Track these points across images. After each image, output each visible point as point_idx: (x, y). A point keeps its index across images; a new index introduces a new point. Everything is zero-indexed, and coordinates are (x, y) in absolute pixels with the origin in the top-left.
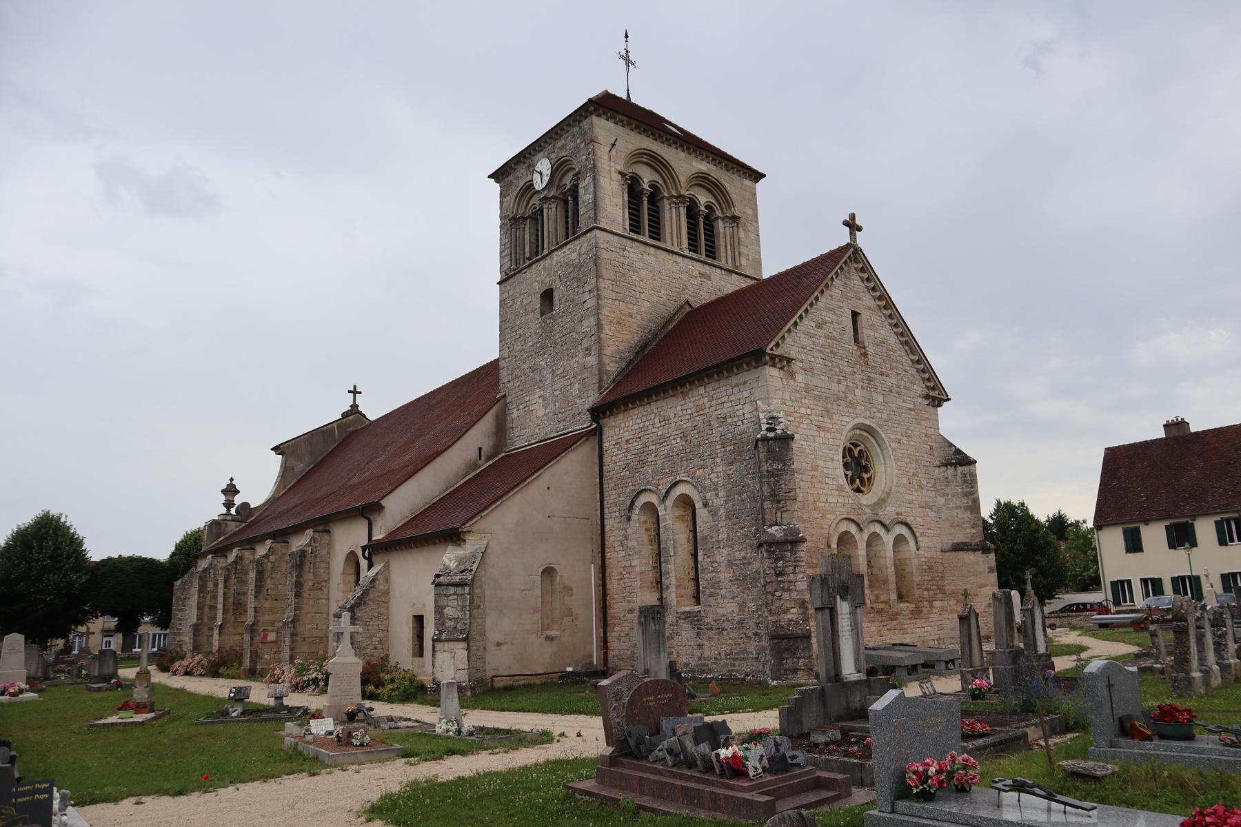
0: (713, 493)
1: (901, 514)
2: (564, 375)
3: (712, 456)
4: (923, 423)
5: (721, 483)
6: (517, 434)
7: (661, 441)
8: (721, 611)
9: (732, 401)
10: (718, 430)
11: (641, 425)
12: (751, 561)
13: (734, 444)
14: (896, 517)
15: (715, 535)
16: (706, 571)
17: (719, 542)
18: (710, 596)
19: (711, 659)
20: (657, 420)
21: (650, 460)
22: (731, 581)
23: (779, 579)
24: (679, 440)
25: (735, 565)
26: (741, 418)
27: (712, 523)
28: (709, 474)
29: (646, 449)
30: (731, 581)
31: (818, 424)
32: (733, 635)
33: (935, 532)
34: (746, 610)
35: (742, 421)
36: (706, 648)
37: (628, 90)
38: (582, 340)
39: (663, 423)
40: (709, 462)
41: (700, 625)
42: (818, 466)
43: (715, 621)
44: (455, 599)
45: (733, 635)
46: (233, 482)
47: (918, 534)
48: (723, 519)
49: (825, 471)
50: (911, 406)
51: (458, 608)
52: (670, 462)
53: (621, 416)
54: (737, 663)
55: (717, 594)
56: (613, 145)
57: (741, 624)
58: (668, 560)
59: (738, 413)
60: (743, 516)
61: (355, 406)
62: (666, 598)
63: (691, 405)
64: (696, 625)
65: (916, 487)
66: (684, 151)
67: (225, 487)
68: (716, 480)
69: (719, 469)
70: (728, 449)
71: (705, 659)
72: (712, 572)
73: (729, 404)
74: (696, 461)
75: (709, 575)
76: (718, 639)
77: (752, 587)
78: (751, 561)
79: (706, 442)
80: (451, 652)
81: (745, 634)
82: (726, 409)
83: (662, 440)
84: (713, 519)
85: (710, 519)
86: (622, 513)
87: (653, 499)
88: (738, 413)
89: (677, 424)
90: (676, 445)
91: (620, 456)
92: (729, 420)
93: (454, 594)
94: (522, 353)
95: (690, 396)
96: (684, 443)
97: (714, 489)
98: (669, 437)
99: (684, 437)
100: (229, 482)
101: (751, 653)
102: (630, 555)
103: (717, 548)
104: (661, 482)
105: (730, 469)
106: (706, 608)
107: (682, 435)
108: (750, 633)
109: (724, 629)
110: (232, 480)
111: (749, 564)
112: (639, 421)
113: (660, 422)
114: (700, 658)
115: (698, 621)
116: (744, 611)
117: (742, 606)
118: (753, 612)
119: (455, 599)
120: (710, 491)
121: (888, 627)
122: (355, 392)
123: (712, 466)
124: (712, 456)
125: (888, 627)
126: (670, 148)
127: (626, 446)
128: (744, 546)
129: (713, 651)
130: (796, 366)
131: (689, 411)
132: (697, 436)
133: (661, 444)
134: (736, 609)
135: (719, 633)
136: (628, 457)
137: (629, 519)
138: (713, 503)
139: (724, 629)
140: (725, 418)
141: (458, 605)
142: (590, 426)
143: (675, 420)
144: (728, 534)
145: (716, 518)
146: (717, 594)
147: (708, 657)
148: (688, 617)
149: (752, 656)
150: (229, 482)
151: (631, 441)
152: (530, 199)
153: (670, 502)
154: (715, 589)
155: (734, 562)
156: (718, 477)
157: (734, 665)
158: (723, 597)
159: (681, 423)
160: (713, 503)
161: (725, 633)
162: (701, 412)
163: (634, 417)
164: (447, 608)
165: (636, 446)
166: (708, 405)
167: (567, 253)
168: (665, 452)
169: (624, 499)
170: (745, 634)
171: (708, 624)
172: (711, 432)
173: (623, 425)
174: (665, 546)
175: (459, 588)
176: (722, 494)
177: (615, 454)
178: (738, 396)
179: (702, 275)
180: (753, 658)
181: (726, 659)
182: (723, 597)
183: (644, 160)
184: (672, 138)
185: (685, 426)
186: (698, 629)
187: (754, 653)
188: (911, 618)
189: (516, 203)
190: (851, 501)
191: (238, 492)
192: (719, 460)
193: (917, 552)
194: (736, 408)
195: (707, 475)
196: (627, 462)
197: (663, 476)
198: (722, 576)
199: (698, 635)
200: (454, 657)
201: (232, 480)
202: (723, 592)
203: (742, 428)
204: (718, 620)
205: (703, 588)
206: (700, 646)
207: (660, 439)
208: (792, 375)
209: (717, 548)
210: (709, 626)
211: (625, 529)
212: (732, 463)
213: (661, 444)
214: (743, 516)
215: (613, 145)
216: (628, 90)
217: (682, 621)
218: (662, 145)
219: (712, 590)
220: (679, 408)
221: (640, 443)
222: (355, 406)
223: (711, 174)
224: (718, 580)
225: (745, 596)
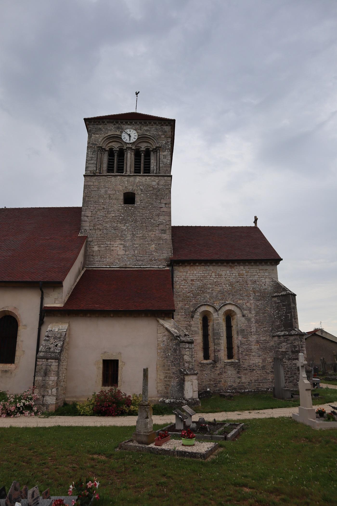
0: (248, 311)
2: (143, 238)
3: (247, 296)
5: (252, 308)
6: (97, 260)
7: (216, 284)
8: (252, 362)
9: (259, 276)
10: (250, 286)
11: (202, 275)
12: (269, 341)
13: (260, 293)
15: (249, 329)
16: (244, 344)
17: (251, 332)
18: (246, 355)
19: (246, 383)
20: (213, 274)
21: (209, 291)
22: (258, 349)
23: (302, 349)
24: (227, 286)
25: (260, 342)
26: (264, 283)
27: (247, 324)
28: (246, 303)
29: (206, 286)
30: (258, 349)
32: (259, 372)
34: (267, 361)
35: (265, 284)
36: (243, 378)
38: (159, 225)
39: (217, 277)
40: (246, 298)
41: (240, 368)
43: (249, 366)
44: (188, 351)
45: (259, 372)
48: (254, 322)
51: (190, 356)
52: (222, 295)
53: (188, 268)
54: (261, 384)
55: (250, 355)
57: (263, 367)
58: (220, 338)
59: (262, 281)
60: (265, 323)
62: (217, 356)
63: (236, 272)
64: (237, 368)
68: (250, 306)
69: (251, 302)
70: (257, 294)
71: (242, 383)
72: (247, 345)
73: (258, 276)
74: (238, 296)
75: (245, 346)
76: (250, 374)
77: (270, 352)
78: (269, 341)
79: (244, 289)
80: (191, 381)
81: (266, 372)
82: (256, 278)
83: (217, 284)
84: (248, 322)
85: (246, 322)
86: (188, 314)
87: (210, 309)
88: (262, 281)
89: (227, 279)
90: (226, 288)
91: (186, 286)
92: (258, 283)
93: (188, 348)
94: (105, 218)
95: (235, 268)
96: (231, 288)
97: (249, 310)
98: (221, 283)
99: (231, 284)
101: (269, 380)
102: (192, 334)
103: (250, 335)
104: (215, 302)
105: (258, 303)
106: (243, 361)
107: (230, 284)
108: (268, 371)
109: (253, 370)
111: (268, 342)
112: (201, 272)
113: (216, 276)
114: (239, 383)
115: (238, 366)
116: (265, 362)
117: (264, 360)
118: (270, 362)
119: (188, 351)
120: (246, 310)
123: (248, 300)
124: (248, 296)
127: (191, 282)
128: (265, 335)
129: (247, 380)
131: (234, 275)
132: (239, 286)
133: (215, 285)
134: (261, 361)
135: (251, 372)
136: (193, 288)
137: (192, 317)
138: (248, 315)
139: (253, 370)
140: (255, 281)
141: (190, 354)
142: (165, 268)
143: (226, 277)
144: (257, 329)
145: (250, 322)
146: (250, 355)
147: (244, 382)
148: (232, 365)
149: (269, 381)
151: (195, 280)
152: (108, 144)
153: (221, 312)
154: (249, 352)
155: (260, 341)
156: (251, 305)
157: (260, 385)
158: (253, 356)
159: (229, 279)
160: (248, 315)
161: (254, 371)
162: (242, 277)
163: (197, 270)
164: (185, 356)
165: (199, 283)
166: (246, 274)
167: (148, 180)
168: (219, 289)
169: (188, 307)
170: (266, 372)
171: (244, 368)
172: (247, 286)
173: (189, 272)
174: (218, 332)
175: (190, 345)
176: (253, 312)
177: (182, 284)
178: (262, 274)
180: (270, 382)
181: (255, 382)
182: (253, 356)
185: (231, 280)
186: (239, 370)
187: (271, 379)
189: (103, 141)
192: (252, 298)
194: (261, 279)
195: (244, 304)
196: (192, 290)
197: (217, 300)
198: (253, 347)
199: (238, 372)
200: (192, 384)
202: (254, 354)
203: (264, 287)
204: (250, 366)
205: (242, 352)
206: (239, 378)
207: (215, 283)
209: (250, 335)
210: (245, 369)
211: (190, 322)
212: (259, 301)
213: (215, 285)
214: (265, 323)
217: (228, 366)
219: (247, 353)
220: (228, 272)
221: (201, 282)
224: (250, 348)
225: (266, 356)
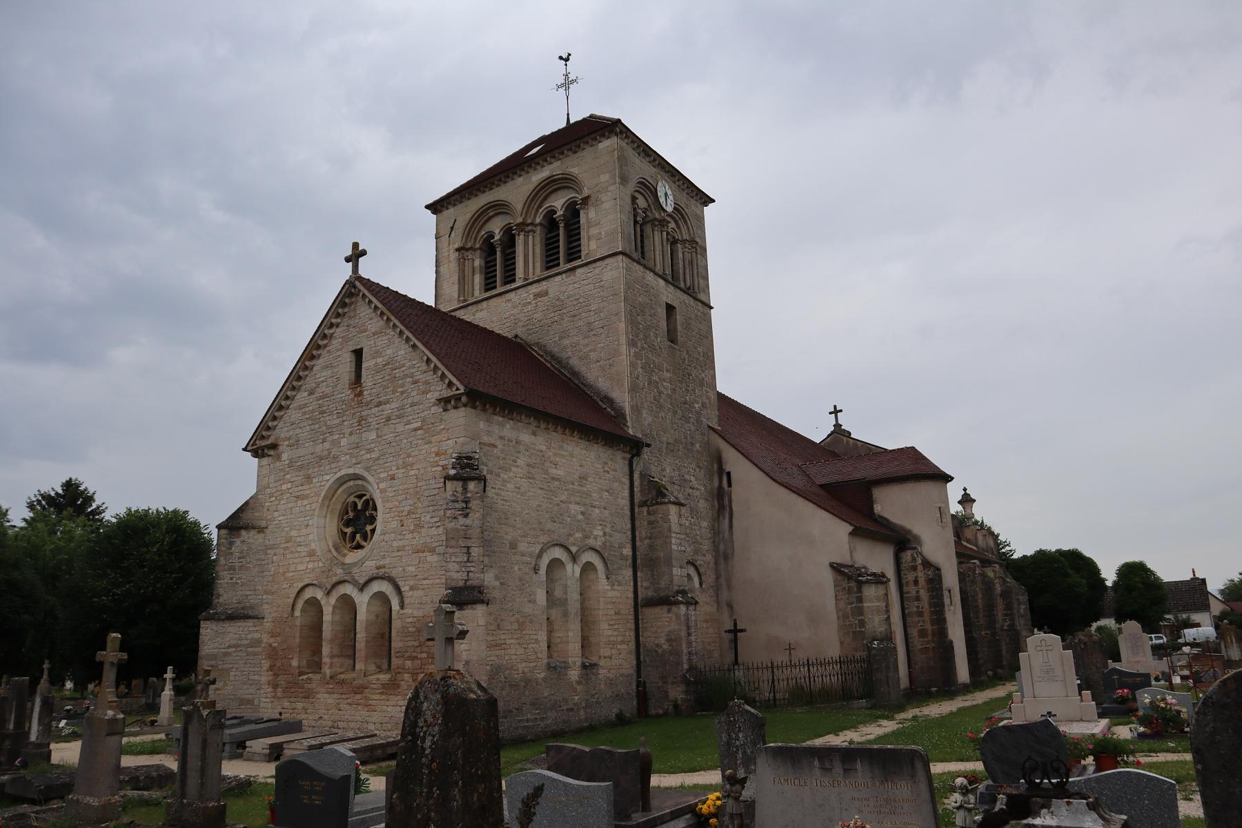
1: (384, 567)
4: (434, 439)
14: (376, 571)
31: (298, 494)
33: (438, 581)
37: (568, 114)
42: (291, 537)
46: (967, 492)
47: (405, 589)
49: (298, 539)
50: (419, 424)
56: (452, 228)
61: (837, 426)
65: (412, 528)
66: (520, 176)
67: (960, 498)
100: (963, 492)
110: (965, 489)
121: (349, 701)
122: (836, 412)
125: (349, 701)
126: (508, 184)
130: (283, 446)
150: (963, 492)
179: (537, 296)
183: (491, 214)
184: (502, 176)
188: (382, 693)
190: (321, 565)
191: (975, 501)
193: (401, 612)
201: (965, 489)
208: (279, 457)
215: (452, 228)
216: (568, 114)
218: (499, 188)
222: (837, 426)
223: (554, 174)
